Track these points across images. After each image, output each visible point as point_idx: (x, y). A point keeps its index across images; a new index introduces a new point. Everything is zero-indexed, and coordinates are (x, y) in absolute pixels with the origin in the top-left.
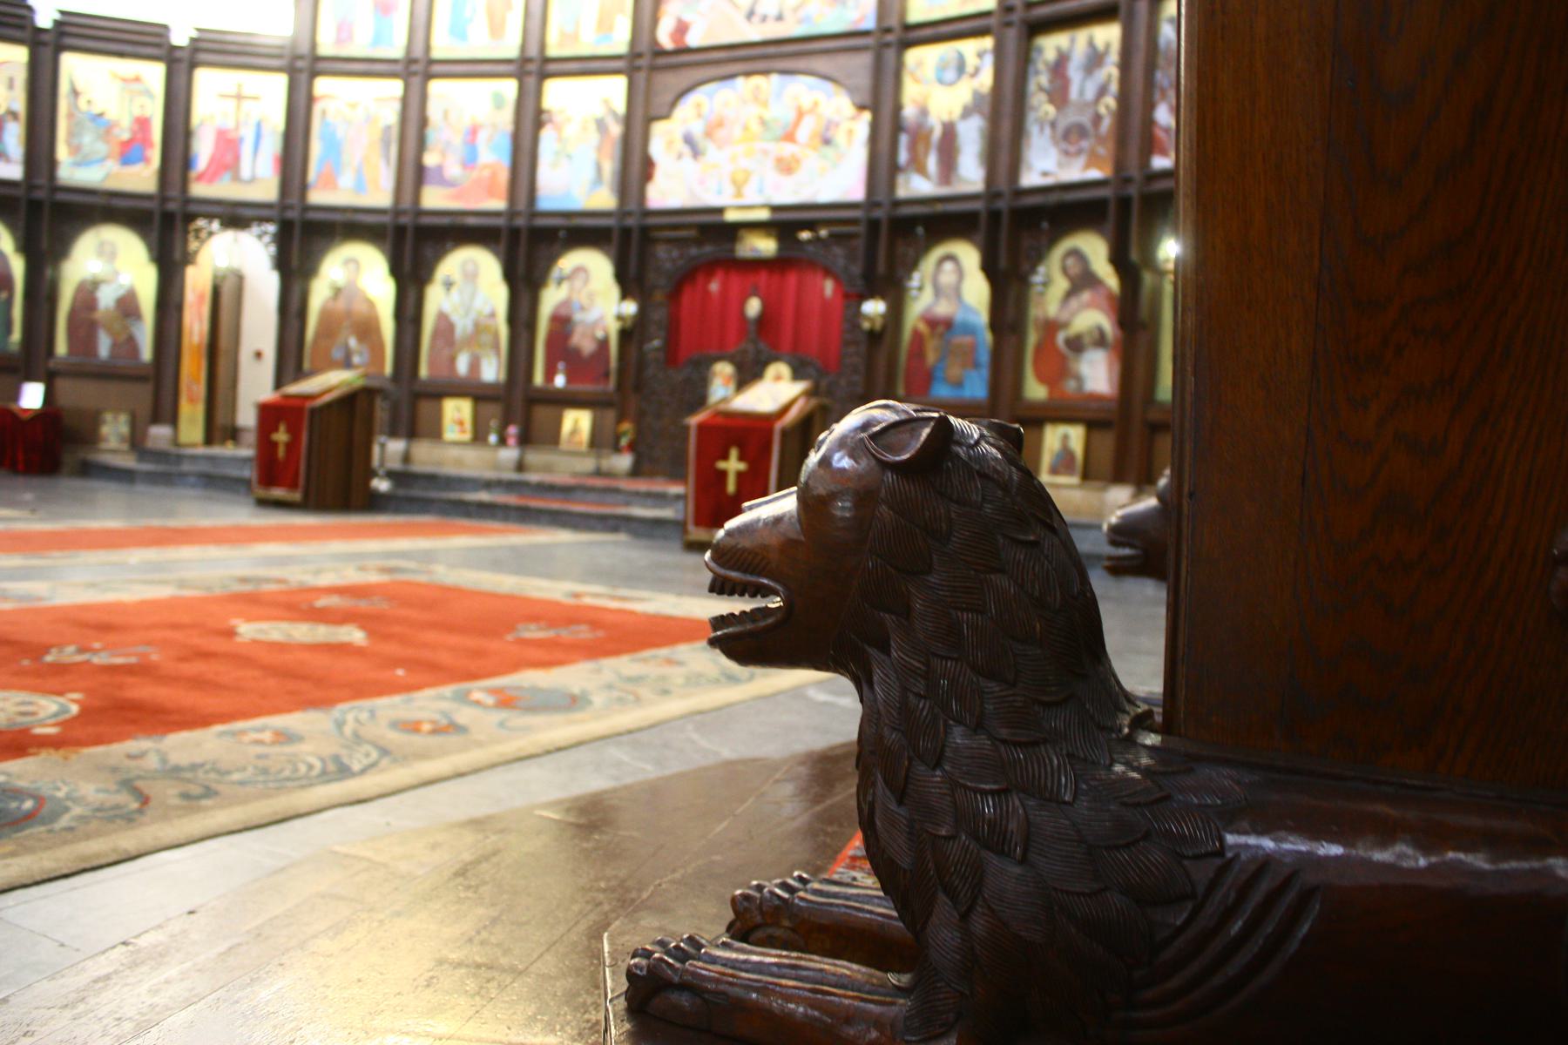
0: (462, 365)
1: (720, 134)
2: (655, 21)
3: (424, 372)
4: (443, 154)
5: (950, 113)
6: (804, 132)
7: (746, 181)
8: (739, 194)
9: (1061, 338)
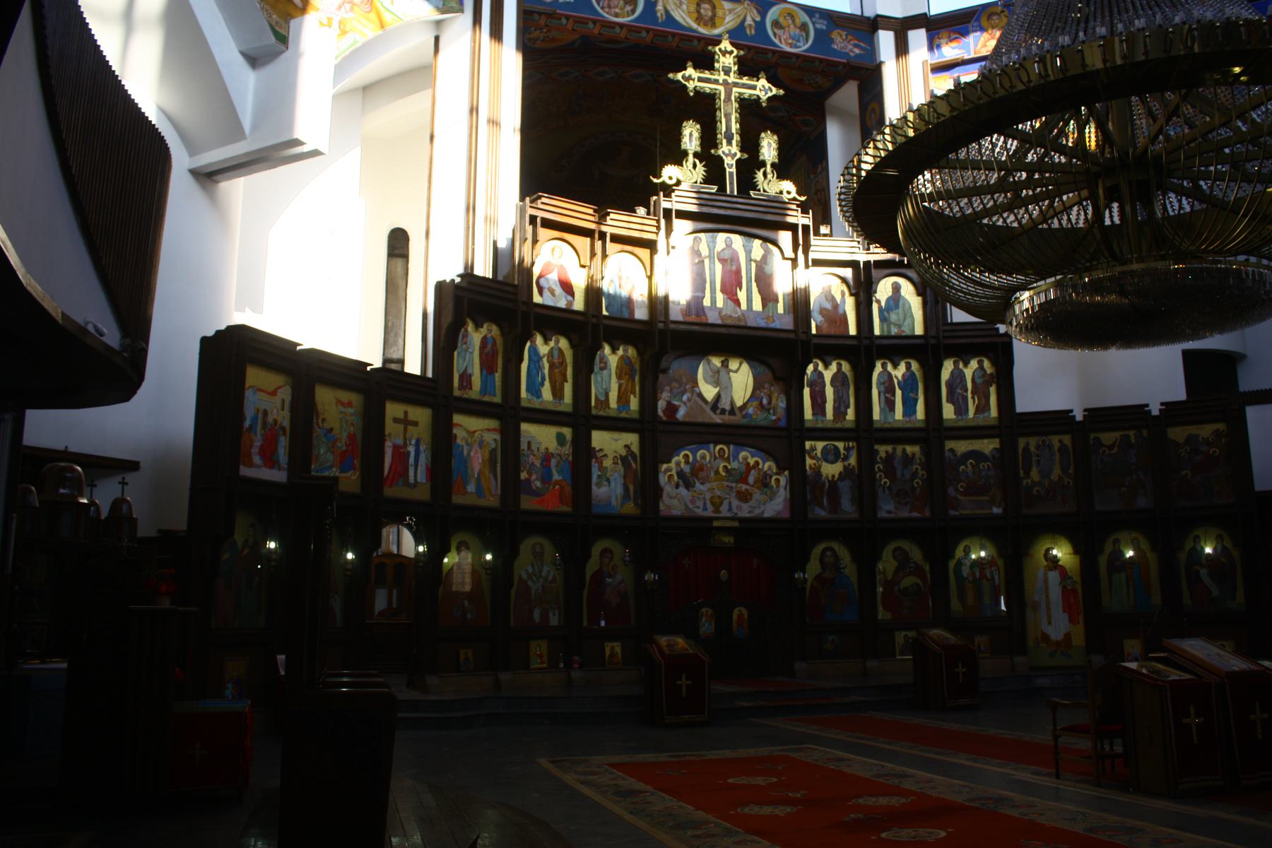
0: (537, 615)
1: (701, 474)
2: (656, 401)
3: (512, 624)
4: (530, 475)
5: (833, 476)
6: (751, 479)
7: (721, 503)
8: (717, 510)
9: (896, 588)
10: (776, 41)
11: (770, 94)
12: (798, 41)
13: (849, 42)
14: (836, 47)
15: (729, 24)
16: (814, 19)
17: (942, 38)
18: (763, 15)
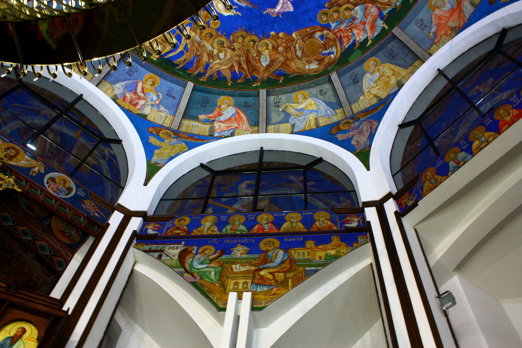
10: (47, 186)
11: (11, 187)
12: (61, 193)
13: (94, 209)
14: (84, 206)
15: (22, 164)
16: (78, 189)
17: (150, 226)
18: (47, 172)
